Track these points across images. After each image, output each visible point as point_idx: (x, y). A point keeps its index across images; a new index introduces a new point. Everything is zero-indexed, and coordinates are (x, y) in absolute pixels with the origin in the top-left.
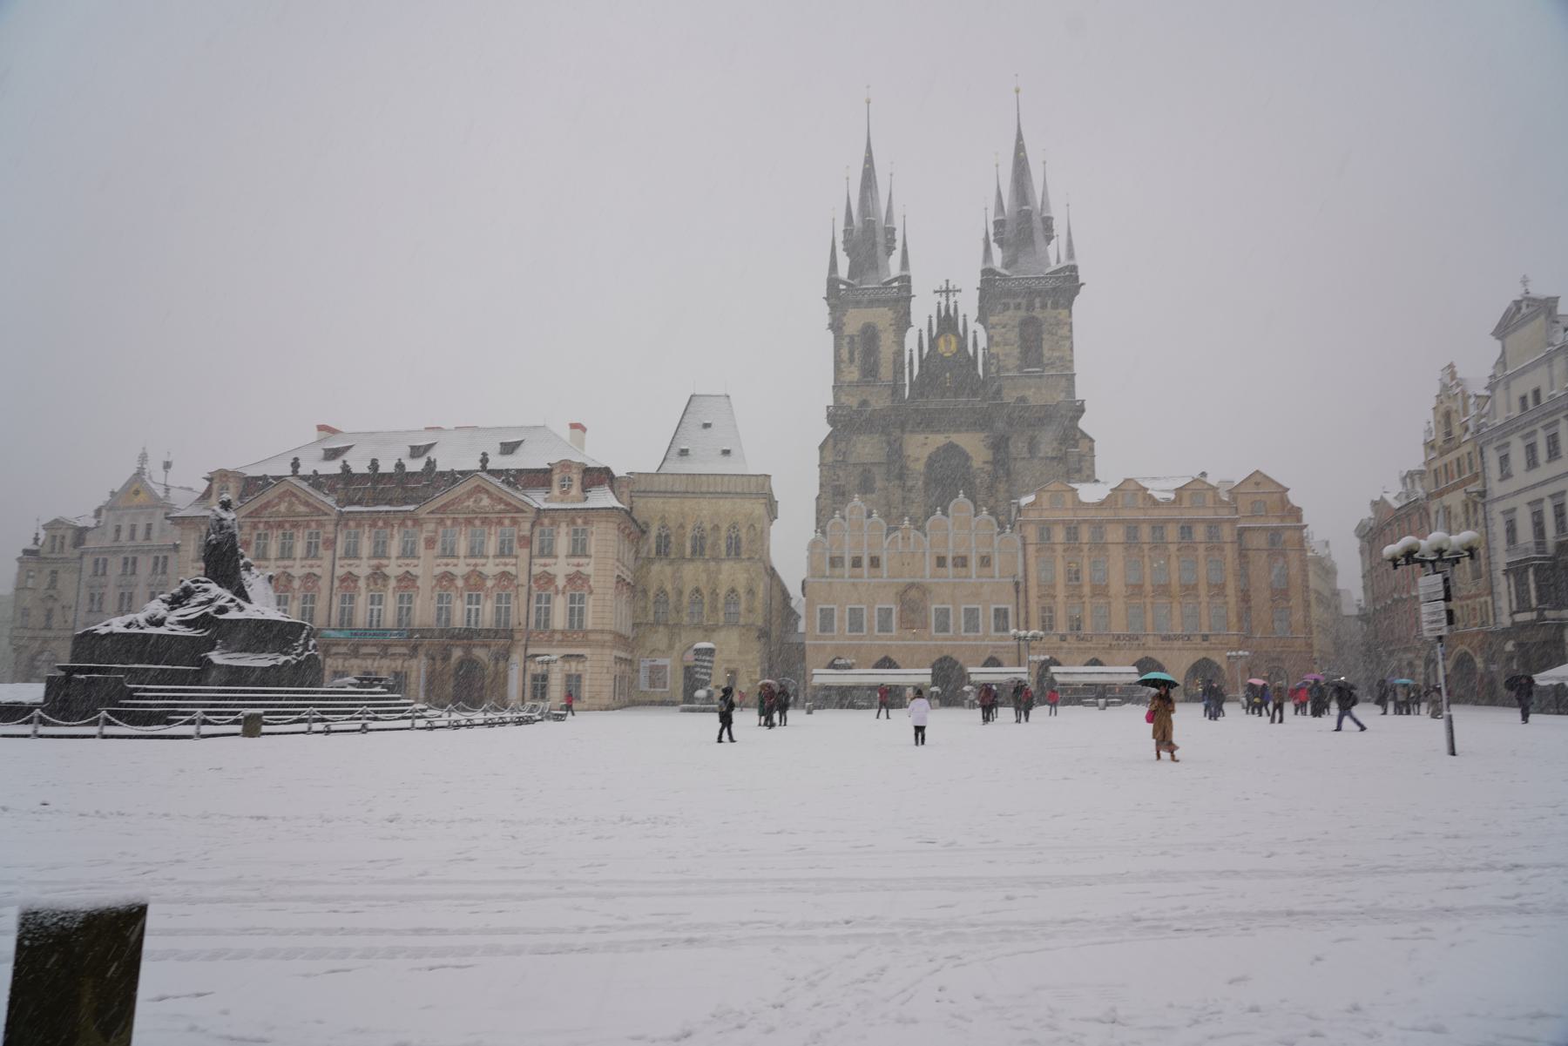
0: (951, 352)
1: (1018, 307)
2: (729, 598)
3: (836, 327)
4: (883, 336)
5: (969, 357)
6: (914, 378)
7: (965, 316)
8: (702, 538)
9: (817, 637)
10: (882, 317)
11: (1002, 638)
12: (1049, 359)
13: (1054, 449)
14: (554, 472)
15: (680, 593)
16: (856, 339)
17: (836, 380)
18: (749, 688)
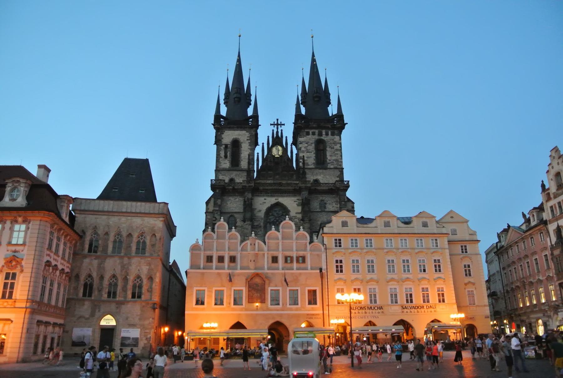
0: (279, 155)
1: (314, 134)
2: (136, 282)
3: (218, 141)
4: (243, 145)
5: (289, 158)
6: (259, 168)
7: (286, 137)
8: (121, 242)
9: (193, 309)
10: (242, 135)
11: (313, 309)
12: (330, 160)
13: (333, 207)
15: (102, 278)
16: (229, 146)
17: (217, 167)
18: (145, 344)
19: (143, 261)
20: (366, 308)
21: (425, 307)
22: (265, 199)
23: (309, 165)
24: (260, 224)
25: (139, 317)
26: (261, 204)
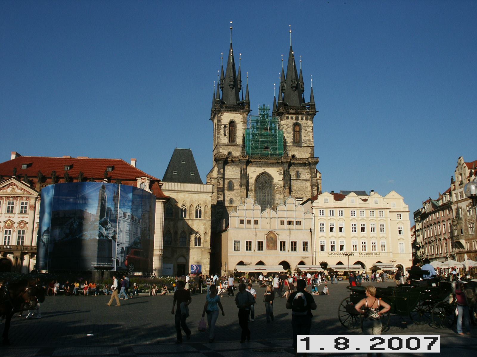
1: (292, 118)
4: (238, 125)
10: (238, 117)
12: (304, 140)
13: (306, 176)
14: (138, 181)
15: (176, 233)
16: (227, 126)
17: (218, 143)
19: (200, 222)
20: (338, 254)
21: (373, 254)
22: (255, 169)
23: (288, 143)
24: (251, 188)
25: (200, 257)
26: (252, 173)
